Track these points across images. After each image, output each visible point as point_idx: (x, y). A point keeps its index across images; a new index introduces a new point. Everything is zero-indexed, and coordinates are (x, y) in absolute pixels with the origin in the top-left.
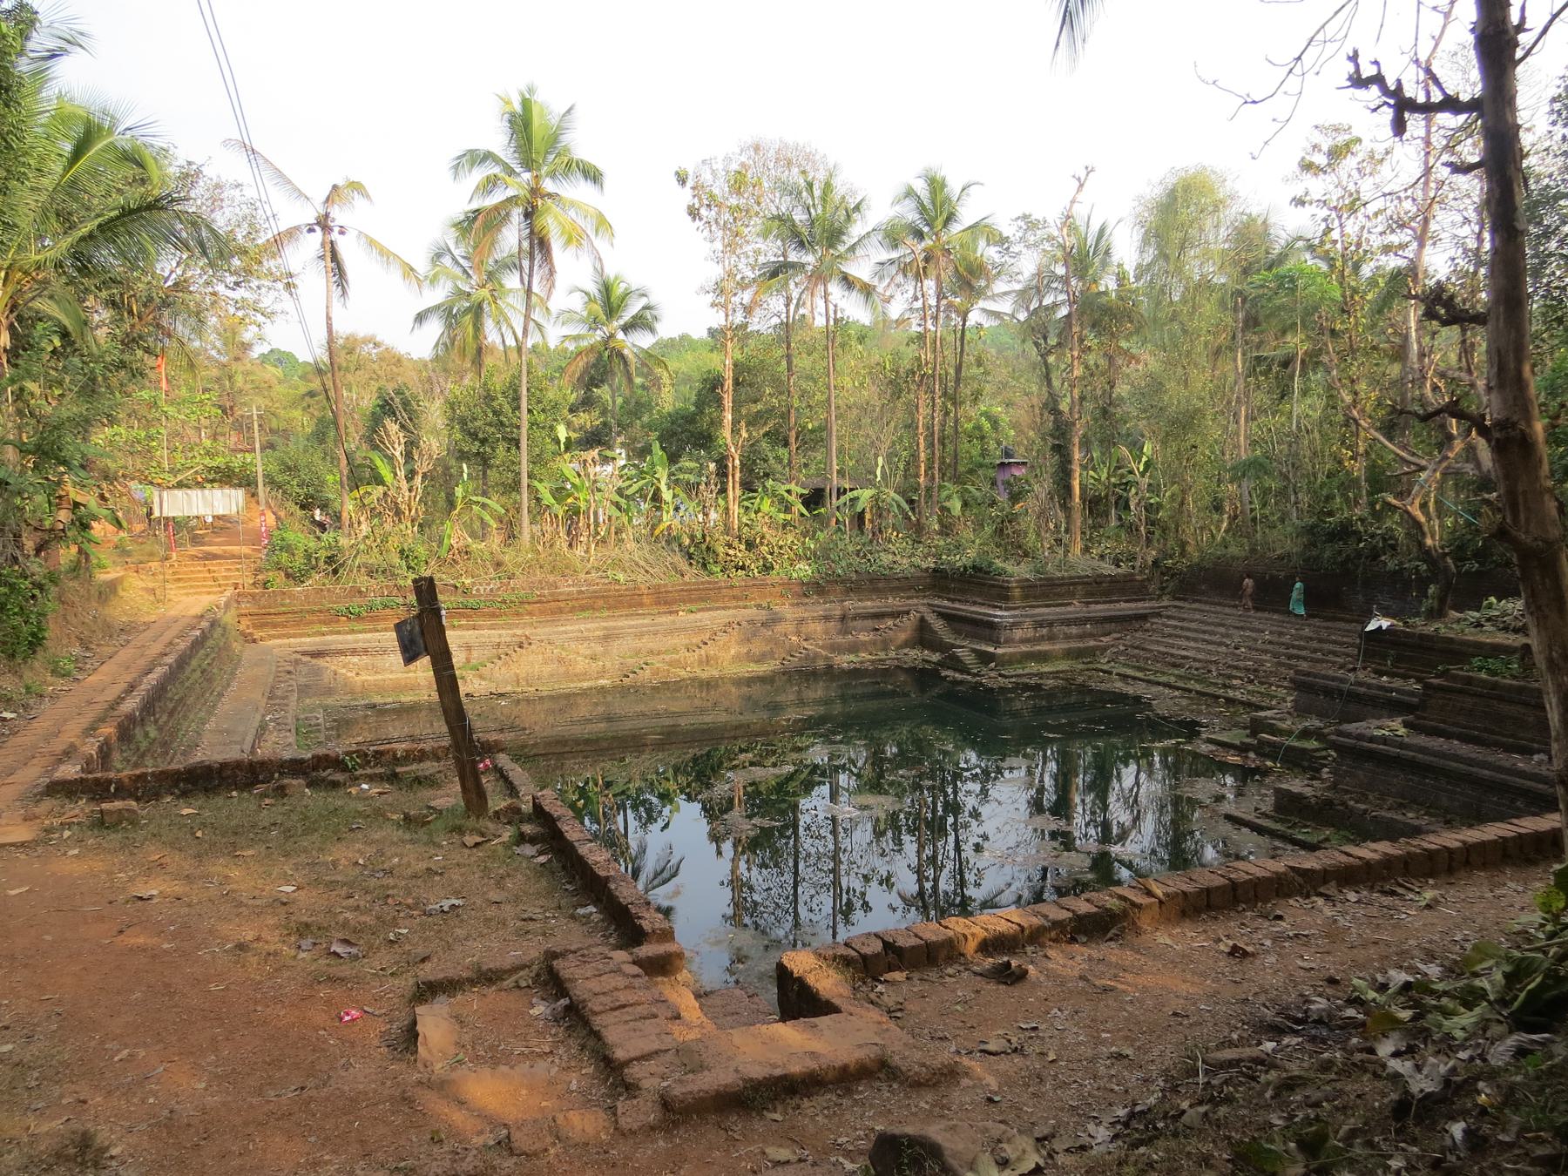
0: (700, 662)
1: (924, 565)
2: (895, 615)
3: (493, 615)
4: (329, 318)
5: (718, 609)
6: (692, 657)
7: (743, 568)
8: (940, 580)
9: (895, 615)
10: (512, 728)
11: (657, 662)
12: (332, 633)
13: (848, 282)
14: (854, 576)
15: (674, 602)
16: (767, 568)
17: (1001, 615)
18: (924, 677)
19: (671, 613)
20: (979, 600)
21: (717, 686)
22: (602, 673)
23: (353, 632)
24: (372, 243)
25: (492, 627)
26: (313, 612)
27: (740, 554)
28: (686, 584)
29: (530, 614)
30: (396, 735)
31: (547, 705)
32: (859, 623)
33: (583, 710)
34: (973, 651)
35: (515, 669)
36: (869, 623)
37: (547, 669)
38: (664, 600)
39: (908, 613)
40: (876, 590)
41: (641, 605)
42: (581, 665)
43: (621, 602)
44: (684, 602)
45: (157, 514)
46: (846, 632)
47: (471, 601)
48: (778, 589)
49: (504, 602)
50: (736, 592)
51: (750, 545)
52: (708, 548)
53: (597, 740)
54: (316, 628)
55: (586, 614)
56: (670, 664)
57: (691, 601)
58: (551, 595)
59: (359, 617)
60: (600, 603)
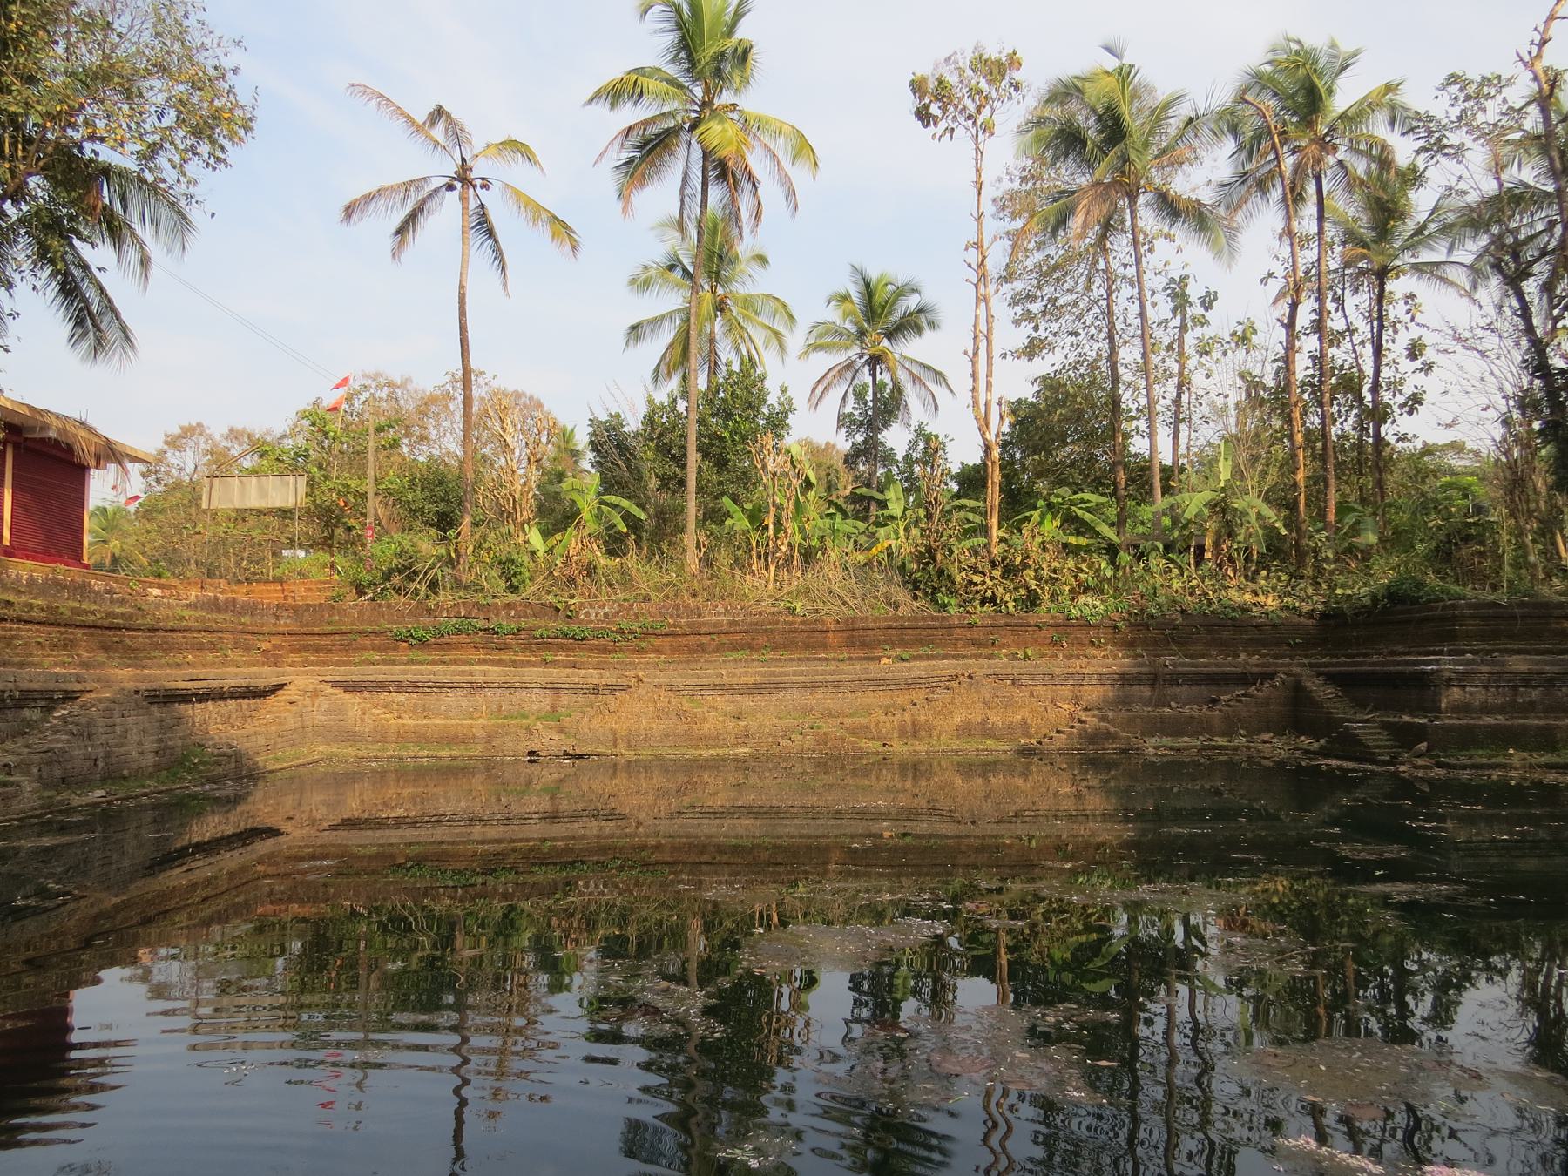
0: (903, 733)
1: (1305, 607)
2: (1244, 680)
3: (605, 650)
4: (462, 287)
5: (945, 657)
6: (889, 724)
7: (993, 600)
8: (1334, 628)
9: (1244, 680)
10: (611, 816)
11: (828, 726)
12: (384, 662)
14: (1179, 620)
15: (876, 644)
16: (1032, 601)
17: (1445, 663)
18: (1303, 783)
19: (868, 659)
20: (1400, 648)
21: (929, 773)
22: (746, 736)
23: (411, 662)
25: (599, 666)
26: (367, 634)
27: (990, 581)
28: (895, 618)
29: (658, 651)
31: (658, 780)
32: (1183, 691)
33: (717, 791)
34: (1386, 726)
35: (611, 722)
36: (1204, 691)
37: (659, 727)
38: (861, 638)
39: (1272, 677)
42: (711, 724)
44: (893, 645)
45: (204, 506)
48: (1052, 632)
49: (621, 631)
50: (975, 633)
51: (1010, 571)
52: (941, 572)
54: (366, 655)
55: (738, 655)
56: (854, 731)
57: (904, 644)
58: (689, 625)
59: (423, 644)
60: (762, 639)
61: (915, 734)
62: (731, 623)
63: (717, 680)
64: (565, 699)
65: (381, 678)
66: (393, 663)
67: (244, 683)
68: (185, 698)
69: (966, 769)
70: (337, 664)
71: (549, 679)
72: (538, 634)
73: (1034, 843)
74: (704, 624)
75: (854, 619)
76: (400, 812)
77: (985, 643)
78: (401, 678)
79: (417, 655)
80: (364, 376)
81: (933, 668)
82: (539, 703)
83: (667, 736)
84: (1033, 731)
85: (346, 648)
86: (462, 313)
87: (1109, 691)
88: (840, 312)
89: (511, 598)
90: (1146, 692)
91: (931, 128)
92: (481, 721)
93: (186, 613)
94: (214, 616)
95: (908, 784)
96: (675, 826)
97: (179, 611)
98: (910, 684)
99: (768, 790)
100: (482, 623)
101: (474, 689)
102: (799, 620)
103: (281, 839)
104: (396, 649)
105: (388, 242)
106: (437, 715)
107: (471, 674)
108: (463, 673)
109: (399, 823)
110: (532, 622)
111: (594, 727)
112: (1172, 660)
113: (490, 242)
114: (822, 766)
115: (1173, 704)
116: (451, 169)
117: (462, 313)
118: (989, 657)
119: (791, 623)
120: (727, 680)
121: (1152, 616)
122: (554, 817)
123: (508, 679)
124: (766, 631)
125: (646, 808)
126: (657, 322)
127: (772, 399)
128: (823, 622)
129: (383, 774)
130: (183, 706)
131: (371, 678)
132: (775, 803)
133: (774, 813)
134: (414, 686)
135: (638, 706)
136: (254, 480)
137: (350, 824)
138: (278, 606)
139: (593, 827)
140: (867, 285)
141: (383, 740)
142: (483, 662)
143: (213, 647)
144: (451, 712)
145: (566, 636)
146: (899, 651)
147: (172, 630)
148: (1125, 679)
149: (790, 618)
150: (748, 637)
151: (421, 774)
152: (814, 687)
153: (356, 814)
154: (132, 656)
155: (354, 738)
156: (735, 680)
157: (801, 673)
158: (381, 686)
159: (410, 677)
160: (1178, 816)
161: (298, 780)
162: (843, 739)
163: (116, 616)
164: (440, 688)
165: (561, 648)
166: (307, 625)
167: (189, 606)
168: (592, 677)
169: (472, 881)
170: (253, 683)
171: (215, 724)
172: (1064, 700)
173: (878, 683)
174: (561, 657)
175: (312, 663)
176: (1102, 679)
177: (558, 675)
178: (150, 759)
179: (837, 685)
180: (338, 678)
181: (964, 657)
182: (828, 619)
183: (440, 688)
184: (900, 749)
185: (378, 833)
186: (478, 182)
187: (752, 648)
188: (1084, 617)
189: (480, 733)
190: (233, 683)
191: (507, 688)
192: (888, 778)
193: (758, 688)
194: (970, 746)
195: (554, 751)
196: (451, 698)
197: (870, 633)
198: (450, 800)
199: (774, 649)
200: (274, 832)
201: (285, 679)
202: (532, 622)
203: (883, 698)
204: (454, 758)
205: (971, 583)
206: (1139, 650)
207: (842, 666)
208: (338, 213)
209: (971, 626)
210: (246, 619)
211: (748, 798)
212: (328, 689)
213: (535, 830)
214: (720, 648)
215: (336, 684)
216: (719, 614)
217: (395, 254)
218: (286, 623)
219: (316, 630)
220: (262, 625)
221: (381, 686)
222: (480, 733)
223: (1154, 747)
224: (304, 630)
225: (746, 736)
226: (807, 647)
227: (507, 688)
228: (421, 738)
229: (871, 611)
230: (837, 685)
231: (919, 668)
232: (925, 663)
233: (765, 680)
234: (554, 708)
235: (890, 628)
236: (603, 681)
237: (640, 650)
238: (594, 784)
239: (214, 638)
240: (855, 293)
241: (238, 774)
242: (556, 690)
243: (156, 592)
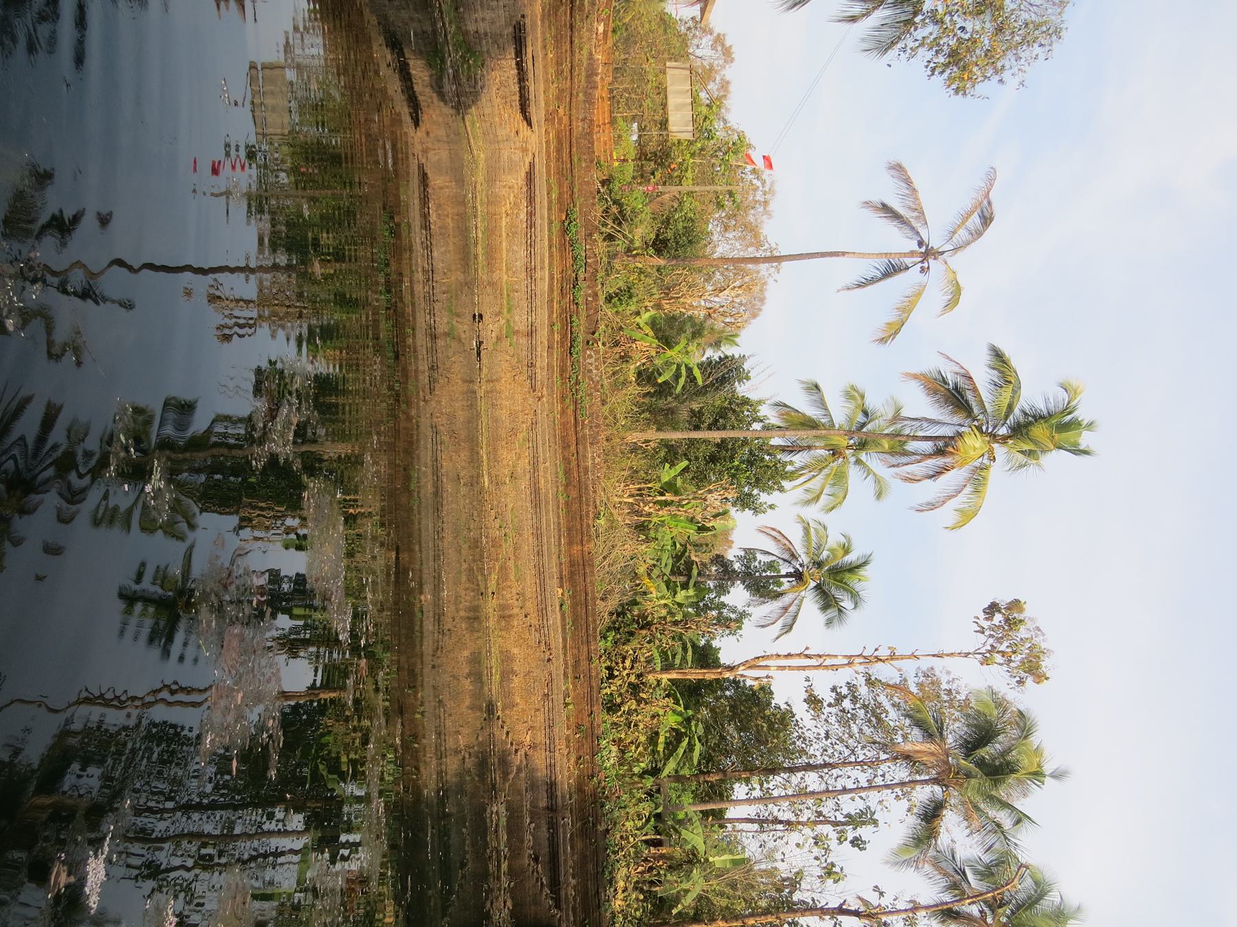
0: (503, 607)
2: (555, 884)
3: (563, 371)
4: (844, 254)
5: (564, 639)
6: (510, 596)
7: (611, 676)
9: (555, 884)
10: (432, 380)
11: (507, 548)
12: (550, 202)
13: (932, 814)
14: (601, 828)
15: (573, 583)
16: (612, 707)
21: (472, 630)
22: (498, 483)
23: (550, 222)
24: (918, 294)
26: (571, 187)
27: (627, 676)
28: (594, 599)
29: (563, 412)
30: (435, 254)
31: (461, 416)
32: (544, 833)
33: (453, 462)
36: (545, 850)
37: (503, 415)
38: (577, 571)
39: (558, 906)
40: (584, 858)
41: (570, 543)
42: (507, 456)
43: (574, 518)
44: (573, 597)
45: (668, 64)
46: (534, 816)
47: (579, 346)
48: (587, 725)
49: (577, 383)
50: (584, 663)
51: (635, 689)
52: (632, 634)
53: (410, 493)
56: (503, 568)
57: (574, 606)
58: (584, 436)
59: (565, 231)
60: (574, 494)
61: (503, 617)
62: (586, 469)
63: (541, 459)
64: (523, 341)
65: (538, 200)
66: (550, 209)
67: (532, 97)
68: (519, 53)
69: (476, 660)
70: (548, 166)
73: (418, 716)
74: (585, 448)
75: (593, 566)
77: (577, 671)
78: (538, 215)
79: (556, 226)
80: (772, 184)
81: (556, 631)
82: (520, 321)
83: (496, 421)
84: (507, 712)
85: (560, 173)
86: (823, 255)
87: (542, 773)
88: (835, 546)
89: (602, 298)
90: (543, 803)
91: (982, 616)
92: (505, 277)
93: (585, 52)
95: (462, 613)
96: (426, 430)
97: (586, 47)
98: (542, 612)
99: (456, 502)
100: (581, 275)
101: (530, 271)
102: (590, 522)
104: (561, 210)
105: (876, 198)
107: (542, 268)
108: (542, 261)
109: (425, 216)
110: (583, 314)
111: (501, 364)
112: (568, 823)
113: (879, 275)
114: (475, 544)
115: (533, 825)
116: (935, 243)
117: (823, 255)
118: (565, 675)
119: (588, 516)
120: (541, 467)
121: (603, 806)
122: (434, 337)
124: (581, 496)
125: (440, 407)
126: (822, 404)
127: (764, 498)
128: (589, 541)
129: (463, 203)
130: (513, 51)
131: (537, 192)
132: (445, 508)
133: (437, 509)
134: (531, 226)
135: (519, 398)
136: (689, 100)
137: (424, 178)
138: (591, 121)
139: (423, 366)
140: (858, 567)
141: (489, 203)
142: (551, 278)
143: (559, 73)
144: (512, 254)
145: (573, 341)
146: (568, 602)
147: (571, 42)
148: (552, 786)
149: (591, 515)
150: (575, 483)
152: (538, 535)
153: (431, 184)
155: (491, 180)
156: (541, 473)
157: (548, 525)
158: (531, 200)
159: (538, 222)
160: (444, 833)
161: (457, 139)
162: (497, 560)
164: (531, 245)
165: (564, 336)
167: (591, 54)
168: (542, 362)
170: (532, 103)
171: (500, 75)
172: (533, 737)
173: (542, 586)
174: (557, 337)
176: (551, 767)
177: (543, 335)
178: (471, 28)
179: (539, 554)
180: (537, 167)
181: (565, 655)
182: (592, 545)
183: (531, 245)
184: (490, 606)
185: (417, 201)
186: (926, 265)
187: (567, 486)
188: (600, 750)
189: (495, 277)
190: (532, 89)
191: (532, 296)
192: (467, 599)
193: (536, 491)
194: (494, 662)
195: (483, 334)
196: (523, 253)
197: (582, 579)
198: (444, 254)
199: (567, 503)
200: (417, 123)
202: (583, 314)
203: (530, 590)
204: (476, 257)
205: (624, 658)
206: (575, 796)
207: (554, 557)
208: (894, 159)
209: (590, 659)
211: (449, 487)
212: (528, 160)
213: (422, 320)
214: (566, 460)
215: (532, 165)
216: (594, 459)
217: (867, 204)
218: (579, 127)
219: (574, 149)
220: (577, 109)
221: (531, 200)
222: (495, 277)
223: (498, 811)
224: (574, 140)
225: (498, 483)
226: (569, 530)
227: (532, 296)
228: (491, 232)
229: (599, 580)
230: (539, 554)
231: (555, 618)
232: (559, 624)
233: (542, 497)
234: (516, 332)
235: (586, 594)
236: (538, 371)
237: (563, 398)
238: (457, 365)
239: (566, 73)
240: (851, 558)
242: (531, 334)
243: (601, 29)
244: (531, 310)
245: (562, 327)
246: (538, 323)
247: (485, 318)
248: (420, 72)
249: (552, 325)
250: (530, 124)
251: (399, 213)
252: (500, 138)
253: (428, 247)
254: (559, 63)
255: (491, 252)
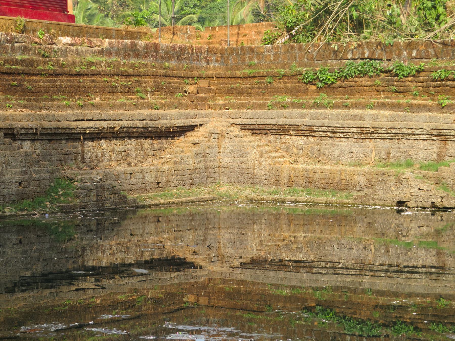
12: (294, 105)
23: (317, 106)
54: (279, 98)
59: (328, 88)
65: (281, 121)
66: (301, 106)
67: (53, 124)
68: (97, 135)
70: (253, 107)
71: (434, 126)
72: (434, 75)
76: (300, 256)
78: (299, 121)
79: (324, 98)
85: (265, 91)
89: (423, 36)
92: (367, 168)
93: (103, 59)
94: (132, 61)
97: (90, 58)
100: (385, 65)
101: (364, 134)
103: (199, 272)
104: (305, 92)
106: (329, 160)
108: (354, 117)
109: (299, 265)
110: (432, 63)
123: (396, 124)
129: (277, 217)
130: (70, 144)
131: (273, 122)
137: (258, 263)
138: (209, 51)
142: (382, 106)
143: (128, 90)
144: (349, 160)
147: (79, 75)
151: (309, 217)
153: (255, 254)
154: (33, 96)
155: (252, 180)
158: (281, 130)
159: (307, 121)
161: (201, 220)
163: (16, 62)
164: (333, 133)
166: (232, 69)
167: (101, 52)
169: (376, 332)
171: (111, 159)
175: (234, 106)
178: (13, 188)
180: (245, 121)
183: (333, 133)
185: (281, 274)
189: (361, 180)
190: (125, 123)
191: (395, 134)
198: (347, 248)
201: (195, 121)
204: (327, 204)
210: (173, 63)
218: (215, 67)
219: (238, 73)
221: (281, 130)
222: (361, 180)
224: (229, 73)
227: (395, 134)
228: (310, 183)
239: (129, 82)
241: (112, 210)
243: (66, 40)
244: (412, 135)
245: (447, 93)
246: (428, 126)
247: (403, 197)
248: (107, 253)
249: (441, 108)
250: (191, 128)
251: (305, 300)
252: (201, 165)
253: (334, 269)
254: (113, 91)
255: (335, 185)
